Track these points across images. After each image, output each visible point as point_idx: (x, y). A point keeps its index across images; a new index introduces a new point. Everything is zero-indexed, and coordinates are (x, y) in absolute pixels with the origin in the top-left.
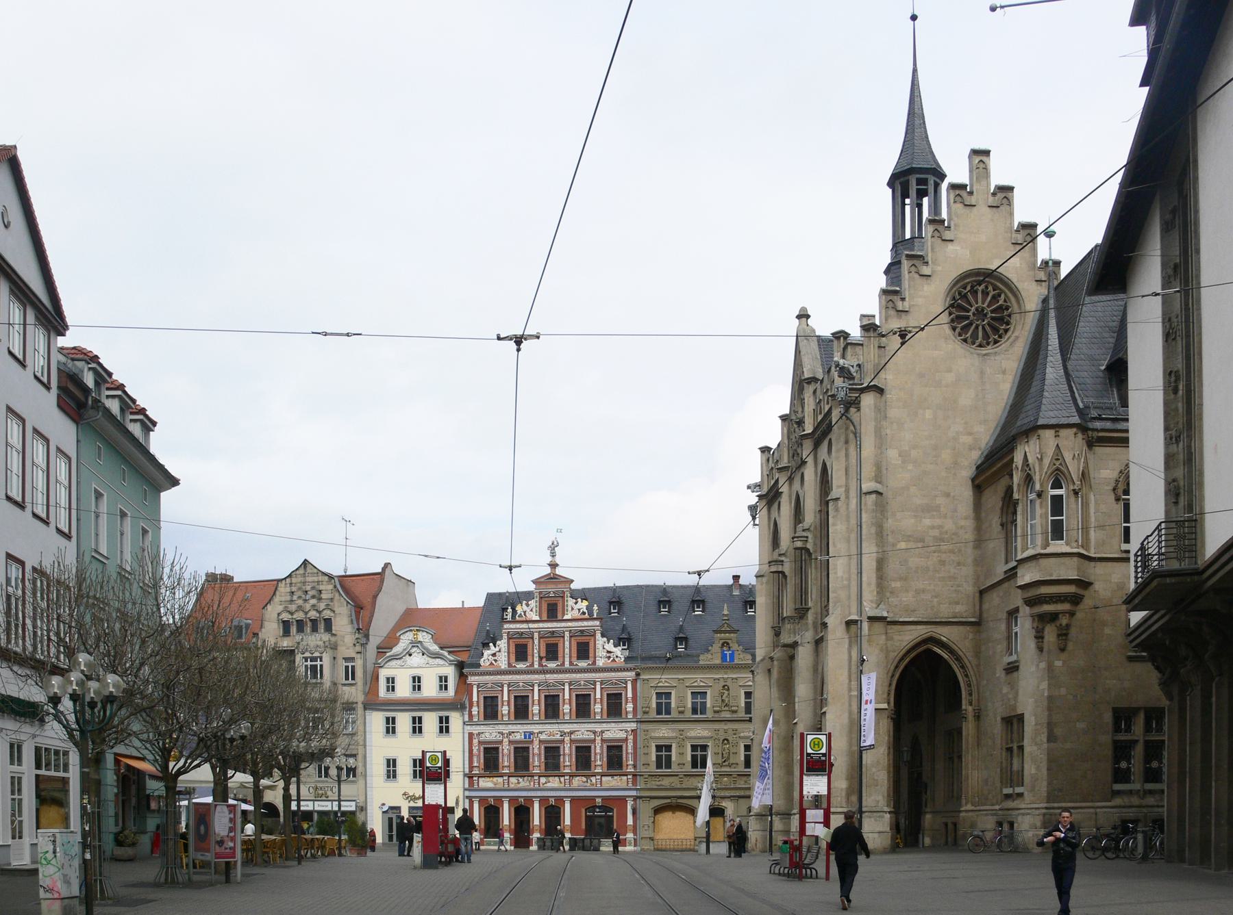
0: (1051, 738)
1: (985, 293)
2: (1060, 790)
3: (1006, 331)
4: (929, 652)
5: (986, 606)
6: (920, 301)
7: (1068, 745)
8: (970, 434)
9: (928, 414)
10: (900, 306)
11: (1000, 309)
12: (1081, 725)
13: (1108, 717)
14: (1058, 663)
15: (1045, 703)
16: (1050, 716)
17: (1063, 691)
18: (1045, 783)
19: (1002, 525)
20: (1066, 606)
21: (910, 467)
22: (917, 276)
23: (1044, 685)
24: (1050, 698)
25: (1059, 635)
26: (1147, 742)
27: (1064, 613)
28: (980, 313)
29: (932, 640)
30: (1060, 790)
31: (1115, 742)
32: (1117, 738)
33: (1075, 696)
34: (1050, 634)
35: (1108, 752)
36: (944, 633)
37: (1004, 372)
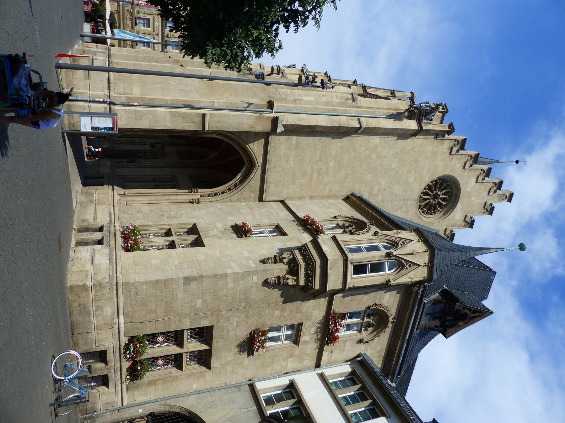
0: (188, 280)
1: (443, 199)
2: (136, 294)
3: (423, 212)
4: (243, 164)
5: (272, 203)
6: (454, 161)
7: (180, 295)
8: (379, 191)
9: (394, 165)
10: (455, 149)
11: (435, 208)
12: (199, 303)
13: (205, 323)
14: (255, 278)
15: (220, 272)
16: (209, 277)
17: (230, 285)
18: (142, 278)
19: (335, 217)
20: (302, 282)
21: (367, 153)
22: (466, 160)
23: (237, 269)
24: (224, 276)
25: (278, 277)
26: (181, 355)
27: (297, 281)
28: (436, 196)
29: (252, 165)
30: (136, 294)
31: (182, 331)
32: (186, 332)
33: (226, 295)
34: (280, 269)
35: (174, 327)
36: (256, 175)
37: (406, 212)
